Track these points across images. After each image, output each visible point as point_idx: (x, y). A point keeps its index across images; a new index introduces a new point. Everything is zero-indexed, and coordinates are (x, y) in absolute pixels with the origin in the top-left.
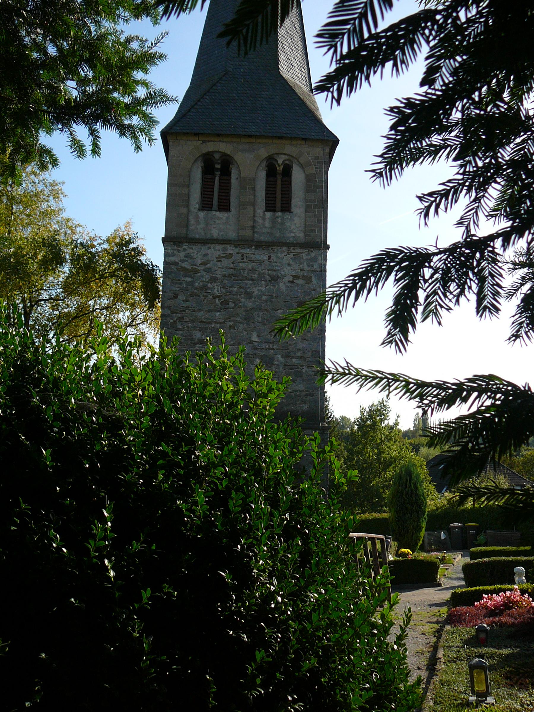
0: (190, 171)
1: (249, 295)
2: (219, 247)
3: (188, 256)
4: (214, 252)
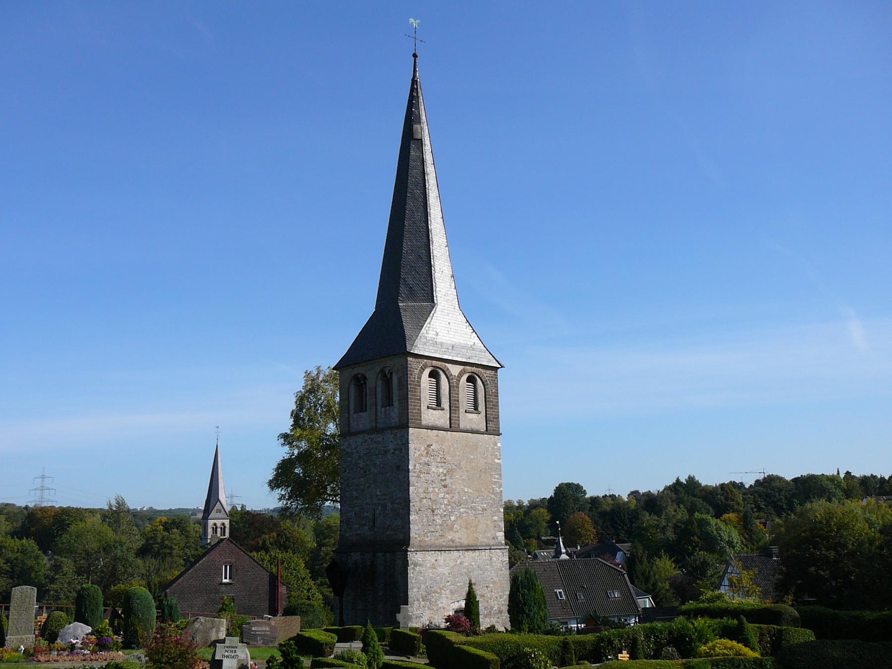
1: (375, 465)
4: (360, 439)
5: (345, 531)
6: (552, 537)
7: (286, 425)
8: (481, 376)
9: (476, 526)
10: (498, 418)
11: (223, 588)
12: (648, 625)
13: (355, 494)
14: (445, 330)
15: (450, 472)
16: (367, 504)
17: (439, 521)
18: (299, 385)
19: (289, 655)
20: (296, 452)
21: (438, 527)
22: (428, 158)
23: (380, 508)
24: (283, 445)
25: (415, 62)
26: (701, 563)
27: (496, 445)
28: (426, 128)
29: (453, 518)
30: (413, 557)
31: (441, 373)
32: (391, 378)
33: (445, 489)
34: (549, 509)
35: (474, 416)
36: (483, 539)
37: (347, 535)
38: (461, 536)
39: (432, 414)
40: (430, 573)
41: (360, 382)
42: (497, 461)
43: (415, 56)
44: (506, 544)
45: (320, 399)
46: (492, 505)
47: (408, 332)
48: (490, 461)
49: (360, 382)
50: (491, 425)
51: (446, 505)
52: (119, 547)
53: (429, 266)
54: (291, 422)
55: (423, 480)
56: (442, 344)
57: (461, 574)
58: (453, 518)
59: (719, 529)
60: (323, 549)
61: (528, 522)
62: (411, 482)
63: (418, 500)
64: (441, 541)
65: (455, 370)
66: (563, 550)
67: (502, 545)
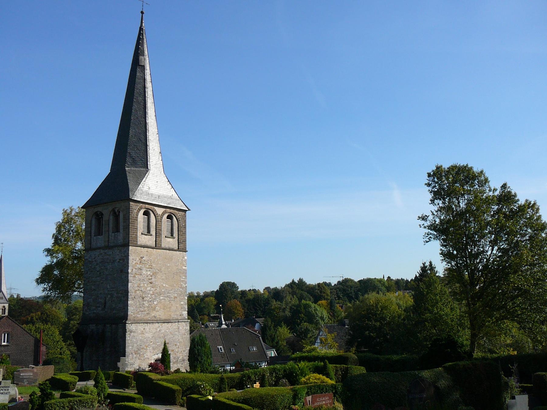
0: (91, 221)
2: (99, 251)
3: (91, 256)
4: (97, 252)
5: (86, 311)
6: (217, 315)
7: (49, 243)
8: (176, 215)
9: (170, 308)
10: (185, 241)
11: (3, 349)
12: (272, 366)
13: (93, 287)
14: (154, 186)
15: (155, 274)
16: (101, 294)
17: (147, 305)
18: (60, 218)
19: (45, 391)
20: (55, 260)
21: (146, 308)
22: (148, 78)
23: (109, 296)
24: (47, 256)
25: (142, 17)
26: (305, 330)
27: (184, 258)
28: (147, 59)
29: (155, 303)
30: (129, 327)
31: (151, 212)
32: (119, 215)
33: (151, 285)
34: (216, 298)
35: (171, 240)
36: (174, 316)
37: (87, 313)
38: (160, 314)
39: (144, 238)
40: (140, 337)
41: (99, 216)
42: (184, 268)
43: (142, 13)
44: (188, 319)
45: (72, 227)
47: (130, 187)
48: (180, 268)
49: (99, 216)
50: (181, 245)
51: (151, 295)
53: (146, 146)
54: (52, 241)
55: (137, 279)
56: (152, 195)
57: (160, 337)
58: (155, 303)
59: (316, 310)
60: (72, 322)
61: (203, 305)
62: (130, 281)
63: (133, 291)
64: (148, 317)
65: (160, 211)
66: (224, 323)
67: (186, 319)
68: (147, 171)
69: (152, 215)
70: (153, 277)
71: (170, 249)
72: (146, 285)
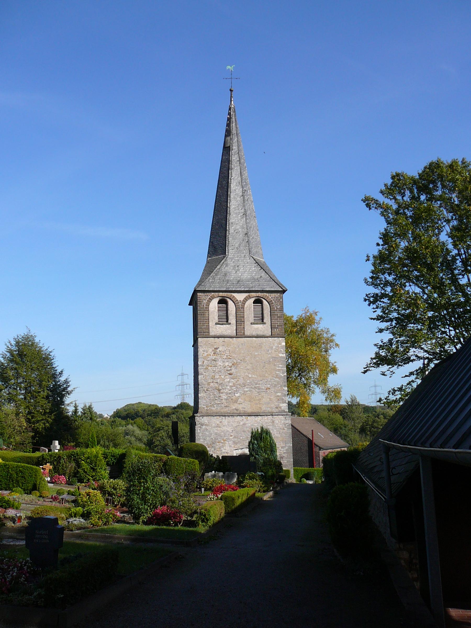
17: (224, 396)
29: (237, 395)
31: (228, 300)
35: (260, 326)
36: (264, 408)
39: (220, 328)
46: (275, 386)
48: (274, 355)
51: (231, 386)
52: (343, 428)
57: (244, 431)
58: (237, 395)
62: (200, 372)
67: (286, 412)
68: (224, 257)
69: (230, 302)
70: (233, 368)
71: (257, 337)
72: (223, 377)
